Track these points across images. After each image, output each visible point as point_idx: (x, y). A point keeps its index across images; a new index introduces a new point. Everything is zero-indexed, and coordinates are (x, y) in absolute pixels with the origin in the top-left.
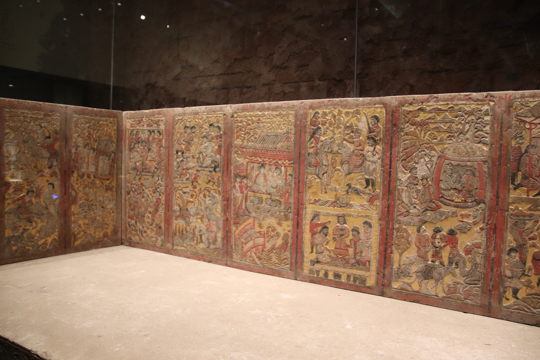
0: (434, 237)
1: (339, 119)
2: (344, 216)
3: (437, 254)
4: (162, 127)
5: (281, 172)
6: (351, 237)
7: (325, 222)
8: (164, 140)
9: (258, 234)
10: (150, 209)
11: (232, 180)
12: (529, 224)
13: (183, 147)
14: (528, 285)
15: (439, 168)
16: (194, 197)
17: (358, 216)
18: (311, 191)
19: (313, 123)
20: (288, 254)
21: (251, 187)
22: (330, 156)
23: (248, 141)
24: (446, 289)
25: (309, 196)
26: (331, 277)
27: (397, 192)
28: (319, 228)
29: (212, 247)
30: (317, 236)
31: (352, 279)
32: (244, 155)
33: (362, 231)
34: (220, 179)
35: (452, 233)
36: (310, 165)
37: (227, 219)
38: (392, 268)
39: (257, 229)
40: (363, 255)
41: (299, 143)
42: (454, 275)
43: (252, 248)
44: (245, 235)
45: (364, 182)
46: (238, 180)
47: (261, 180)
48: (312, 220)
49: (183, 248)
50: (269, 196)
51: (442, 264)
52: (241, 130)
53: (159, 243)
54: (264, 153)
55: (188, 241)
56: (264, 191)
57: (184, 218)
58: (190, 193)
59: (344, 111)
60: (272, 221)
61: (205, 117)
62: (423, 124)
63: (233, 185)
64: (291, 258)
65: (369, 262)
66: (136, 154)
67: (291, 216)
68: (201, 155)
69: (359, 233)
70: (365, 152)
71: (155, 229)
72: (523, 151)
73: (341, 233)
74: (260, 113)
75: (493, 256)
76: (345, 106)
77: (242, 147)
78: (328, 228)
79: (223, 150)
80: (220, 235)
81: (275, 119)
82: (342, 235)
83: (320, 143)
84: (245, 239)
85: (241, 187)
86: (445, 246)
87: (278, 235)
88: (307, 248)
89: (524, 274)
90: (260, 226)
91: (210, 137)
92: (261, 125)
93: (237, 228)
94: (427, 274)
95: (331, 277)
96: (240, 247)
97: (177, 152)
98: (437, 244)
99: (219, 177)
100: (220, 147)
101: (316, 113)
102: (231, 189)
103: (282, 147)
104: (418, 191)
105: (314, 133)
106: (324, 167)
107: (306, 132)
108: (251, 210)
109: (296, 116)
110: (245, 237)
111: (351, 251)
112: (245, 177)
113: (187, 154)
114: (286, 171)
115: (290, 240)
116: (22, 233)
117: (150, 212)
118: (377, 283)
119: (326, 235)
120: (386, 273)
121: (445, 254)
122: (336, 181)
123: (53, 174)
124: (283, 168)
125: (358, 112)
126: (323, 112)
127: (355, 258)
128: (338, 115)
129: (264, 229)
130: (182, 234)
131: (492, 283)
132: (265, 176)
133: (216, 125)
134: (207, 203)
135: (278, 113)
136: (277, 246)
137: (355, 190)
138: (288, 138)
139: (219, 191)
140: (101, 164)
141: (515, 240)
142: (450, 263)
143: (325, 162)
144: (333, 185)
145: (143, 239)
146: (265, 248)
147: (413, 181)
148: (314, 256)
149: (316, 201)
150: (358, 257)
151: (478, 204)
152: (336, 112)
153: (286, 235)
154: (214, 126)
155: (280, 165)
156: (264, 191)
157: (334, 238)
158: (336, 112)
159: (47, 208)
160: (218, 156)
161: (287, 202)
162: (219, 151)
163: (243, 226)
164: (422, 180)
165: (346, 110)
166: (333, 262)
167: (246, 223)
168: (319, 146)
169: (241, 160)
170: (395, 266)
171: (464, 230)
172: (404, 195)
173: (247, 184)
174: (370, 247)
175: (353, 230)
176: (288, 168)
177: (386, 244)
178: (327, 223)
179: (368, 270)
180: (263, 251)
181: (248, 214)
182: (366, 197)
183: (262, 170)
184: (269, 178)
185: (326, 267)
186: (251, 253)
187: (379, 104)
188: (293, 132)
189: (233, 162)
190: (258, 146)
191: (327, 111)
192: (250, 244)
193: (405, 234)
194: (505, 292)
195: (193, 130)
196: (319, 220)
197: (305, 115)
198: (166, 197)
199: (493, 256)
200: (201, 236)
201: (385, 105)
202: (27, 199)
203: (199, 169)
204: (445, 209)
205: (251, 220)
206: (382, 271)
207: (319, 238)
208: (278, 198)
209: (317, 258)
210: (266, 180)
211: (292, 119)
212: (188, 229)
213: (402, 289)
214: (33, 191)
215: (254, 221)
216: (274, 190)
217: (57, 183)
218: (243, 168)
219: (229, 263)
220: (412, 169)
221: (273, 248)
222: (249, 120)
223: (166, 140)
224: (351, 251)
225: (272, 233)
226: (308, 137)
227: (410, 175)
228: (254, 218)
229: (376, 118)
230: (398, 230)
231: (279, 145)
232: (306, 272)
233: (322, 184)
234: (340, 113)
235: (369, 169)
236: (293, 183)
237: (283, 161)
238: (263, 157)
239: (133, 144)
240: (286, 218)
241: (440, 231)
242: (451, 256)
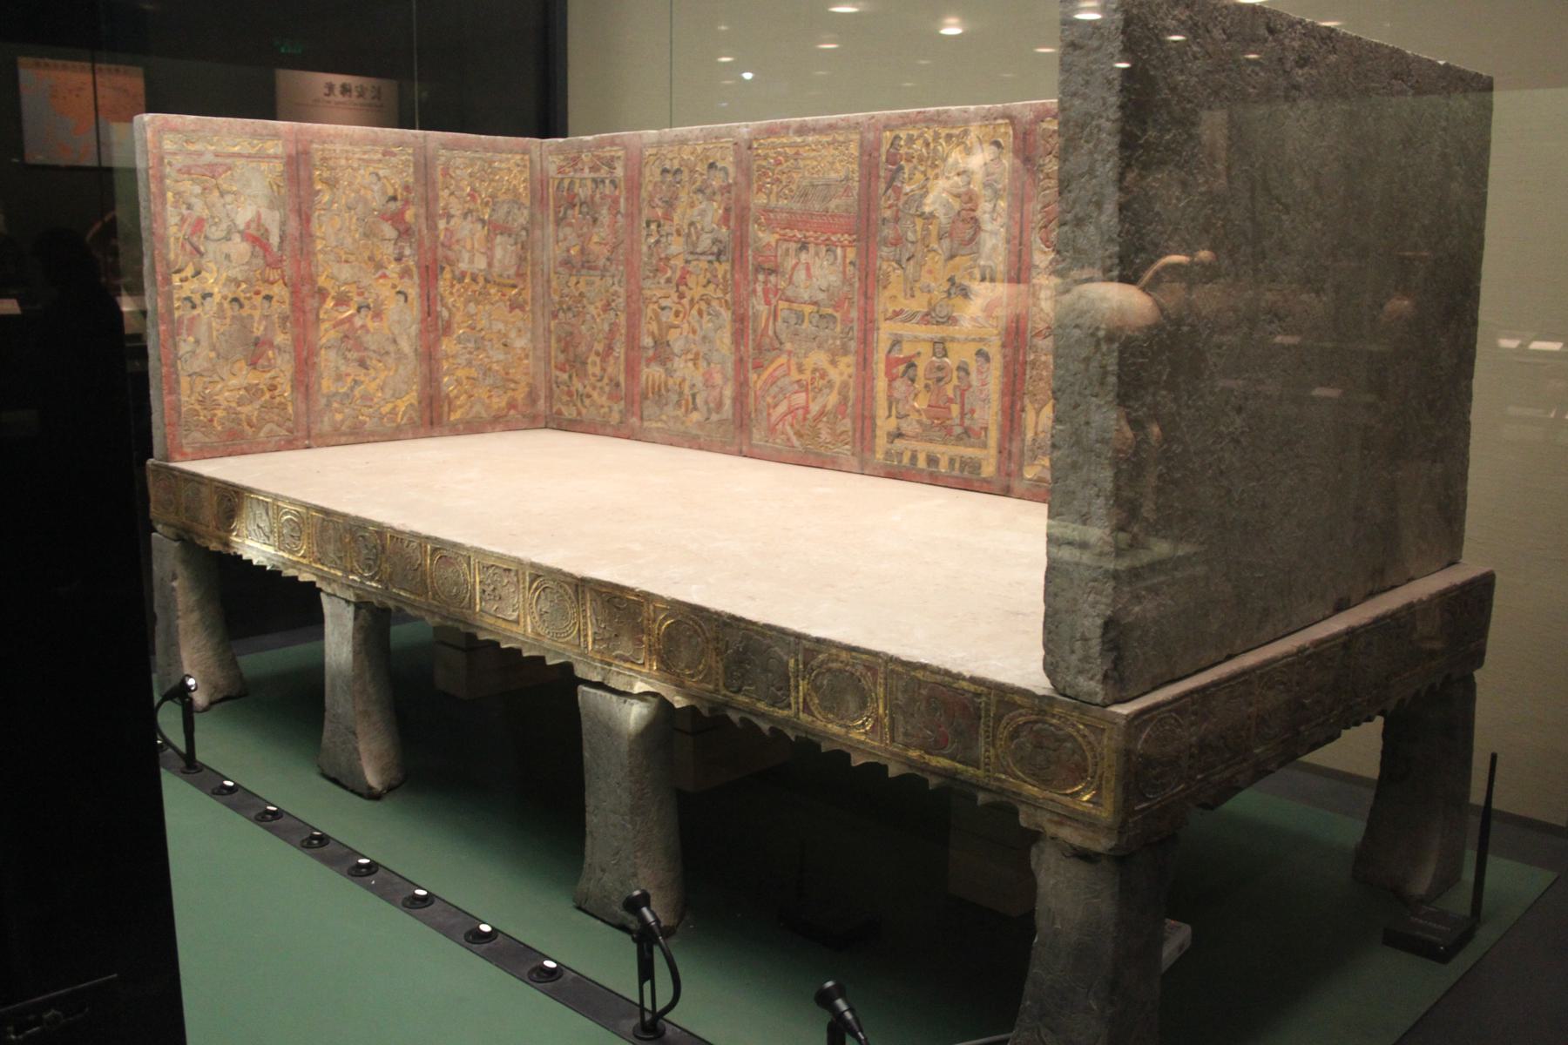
1: (935, 149)
2: (942, 341)
4: (619, 172)
6: (955, 381)
8: (622, 200)
9: (796, 387)
11: (751, 277)
13: (660, 212)
17: (967, 340)
18: (887, 293)
19: (893, 159)
20: (847, 424)
21: (783, 291)
22: (919, 222)
23: (778, 196)
25: (883, 303)
26: (922, 463)
28: (902, 368)
29: (715, 417)
30: (898, 383)
31: (957, 465)
32: (769, 226)
33: (973, 368)
36: (885, 242)
39: (795, 376)
41: (867, 201)
44: (774, 390)
46: (761, 277)
47: (801, 275)
49: (660, 425)
52: (765, 174)
53: (615, 418)
55: (670, 410)
56: (806, 297)
57: (663, 363)
59: (944, 132)
60: (819, 358)
61: (699, 149)
64: (854, 430)
65: (986, 429)
66: (568, 230)
67: (853, 345)
69: (968, 373)
70: (978, 214)
71: (607, 389)
73: (939, 375)
74: (799, 140)
76: (944, 124)
77: (767, 210)
79: (733, 215)
80: (728, 392)
81: (824, 152)
82: (939, 380)
83: (903, 199)
85: (766, 292)
87: (830, 384)
88: (881, 411)
90: (800, 370)
91: (708, 191)
95: (922, 463)
100: (727, 210)
101: (897, 137)
102: (748, 295)
105: (893, 179)
107: (878, 177)
108: (783, 337)
109: (861, 146)
111: (955, 409)
112: (773, 271)
113: (666, 228)
114: (845, 257)
115: (852, 394)
116: (352, 389)
117: (598, 354)
118: (999, 469)
119: (913, 381)
120: (1015, 450)
122: (930, 272)
123: (405, 273)
124: (839, 251)
127: (962, 424)
129: (807, 376)
130: (658, 393)
132: (808, 269)
135: (829, 139)
136: (829, 407)
138: (847, 189)
140: (499, 253)
143: (910, 236)
144: (926, 279)
145: (584, 411)
148: (892, 424)
149: (897, 314)
150: (967, 422)
152: (929, 136)
153: (845, 385)
156: (806, 297)
157: (927, 386)
158: (929, 136)
159: (395, 341)
160: (724, 230)
161: (846, 320)
162: (725, 219)
163: (770, 370)
165: (947, 131)
166: (925, 435)
167: (774, 365)
168: (900, 204)
169: (767, 238)
170: (1030, 435)
174: (986, 400)
175: (959, 368)
177: (1013, 394)
179: (984, 446)
180: (805, 419)
183: (804, 256)
184: (815, 271)
185: (914, 445)
187: (1003, 117)
188: (856, 176)
189: (751, 241)
190: (796, 206)
191: (915, 133)
192: (782, 408)
195: (678, 177)
196: (901, 351)
197: (879, 142)
198: (628, 320)
200: (694, 396)
201: (1011, 119)
202: (358, 322)
203: (690, 257)
205: (783, 359)
207: (901, 386)
208: (830, 311)
210: (809, 275)
211: (854, 149)
212: (671, 382)
214: (368, 307)
217: (413, 292)
219: (745, 448)
221: (822, 413)
222: (779, 154)
223: (627, 199)
226: (883, 186)
228: (790, 353)
230: (1033, 363)
231: (832, 205)
232: (880, 456)
233: (906, 279)
234: (937, 136)
238: (805, 229)
240: (846, 353)
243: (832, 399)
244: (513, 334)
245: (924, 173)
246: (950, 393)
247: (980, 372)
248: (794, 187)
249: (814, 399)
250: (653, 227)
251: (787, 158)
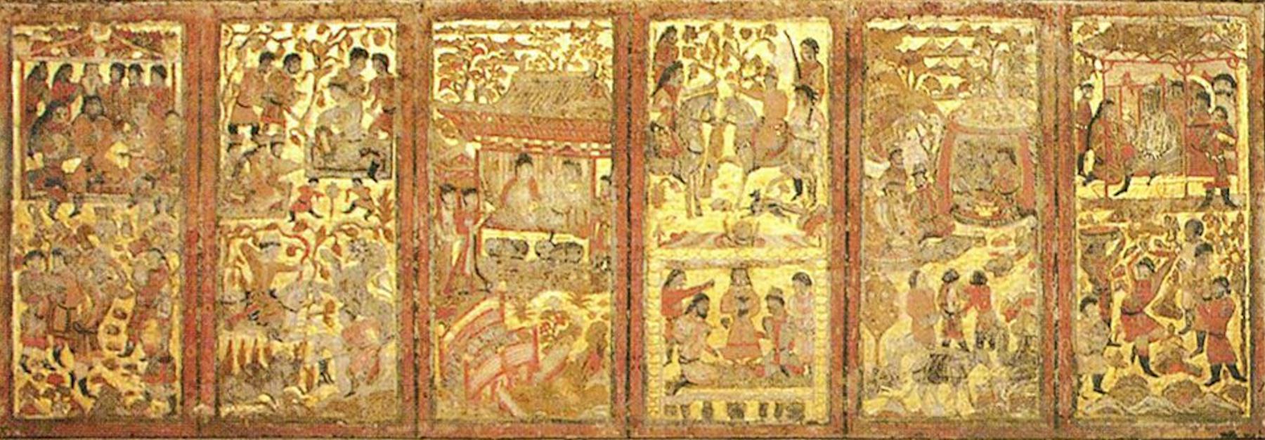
0: (944, 290)
3: (952, 328)
5: (579, 172)
6: (765, 312)
7: (701, 283)
9: (516, 337)
10: (118, 303)
12: (1111, 248)
13: (258, 110)
14: (1118, 363)
15: (946, 146)
16: (300, 254)
18: (660, 214)
24: (975, 398)
27: (864, 203)
28: (686, 302)
31: (771, 410)
34: (392, 196)
35: (979, 279)
37: (415, 308)
38: (861, 372)
40: (795, 350)
41: (627, 99)
42: (987, 363)
43: (501, 373)
45: (790, 183)
48: (667, 283)
50: (547, 237)
51: (964, 347)
52: (454, 65)
54: (532, 125)
55: (276, 387)
56: (532, 221)
58: (285, 247)
59: (738, 25)
62: (912, 59)
63: (434, 212)
68: (323, 137)
69: (782, 302)
71: (142, 367)
72: (1094, 111)
75: (1056, 317)
78: (707, 298)
79: (397, 119)
80: (390, 353)
82: (742, 313)
84: (477, 355)
85: (459, 219)
86: (966, 309)
87: (575, 331)
89: (1110, 344)
92: (518, 54)
93: (448, 329)
94: (935, 372)
96: (461, 378)
97: (233, 129)
98: (951, 309)
99: (386, 192)
103: (580, 110)
104: (907, 198)
106: (694, 156)
110: (475, 350)
111: (767, 345)
119: (704, 316)
124: (584, 164)
125: (771, 30)
126: (687, 27)
128: (724, 34)
129: (537, 321)
131: (1056, 372)
133: (373, 49)
134: (344, 266)
137: (771, 206)
138: (596, 90)
139: (387, 233)
141: (1090, 280)
142: (980, 343)
143: (695, 146)
146: (539, 369)
148: (673, 371)
150: (783, 360)
151: (1023, 216)
152: (718, 27)
153: (597, 333)
154: (366, 55)
155: (576, 155)
157: (723, 321)
162: (386, 120)
164: (914, 175)
167: (477, 311)
170: (868, 366)
171: (1000, 271)
172: (879, 209)
173: (477, 210)
175: (768, 298)
176: (599, 162)
178: (705, 286)
179: (810, 383)
181: (483, 287)
182: (795, 217)
183: (525, 170)
186: (493, 389)
189: (431, 152)
191: (697, 24)
193: (885, 295)
194: (1080, 384)
199: (1056, 317)
200: (324, 366)
205: (492, 303)
206: (841, 381)
207: (685, 325)
208: (572, 238)
209: (683, 376)
211: (606, 39)
213: (886, 414)
215: (502, 305)
218: (464, 168)
220: (894, 154)
221: (563, 367)
224: (767, 345)
225: (560, 327)
226: (652, 86)
227: (888, 164)
229: (812, 45)
234: (729, 30)
235: (800, 155)
236: (614, 197)
237: (584, 146)
239: (41, 109)
241: (956, 279)
242: (980, 329)
243: (580, 346)
245: (712, 72)
246: (759, 328)
247: (799, 298)
248: (506, 82)
249: (547, 350)
250: (245, 131)
251: (492, 46)
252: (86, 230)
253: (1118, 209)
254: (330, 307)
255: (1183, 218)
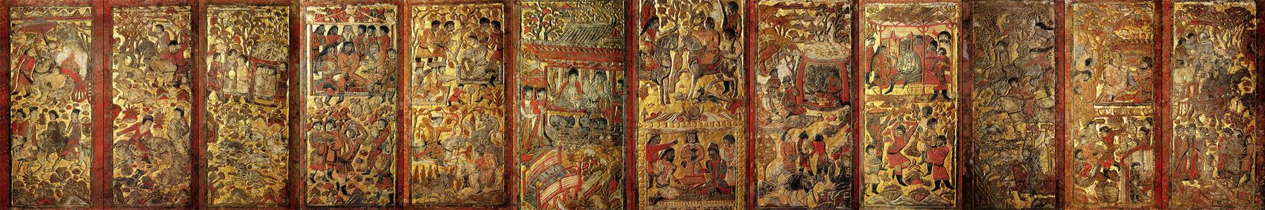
3: (805, 160)
35: (819, 138)
42: (824, 181)
51: (811, 173)
62: (783, 21)
71: (376, 180)
94: (795, 184)
104: (780, 95)
121: (814, 160)
142: (819, 171)
147: (774, 82)
151: (843, 105)
170: (760, 182)
171: (831, 132)
172: (764, 101)
195: (450, 27)
204: (810, 113)
210: (580, 92)
216: (593, 105)
230: (760, 140)
244: (271, 143)
252: (346, 111)
253: (888, 100)
254: (469, 149)
255: (921, 105)
